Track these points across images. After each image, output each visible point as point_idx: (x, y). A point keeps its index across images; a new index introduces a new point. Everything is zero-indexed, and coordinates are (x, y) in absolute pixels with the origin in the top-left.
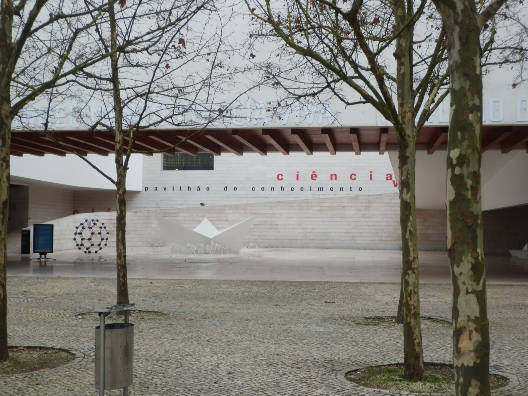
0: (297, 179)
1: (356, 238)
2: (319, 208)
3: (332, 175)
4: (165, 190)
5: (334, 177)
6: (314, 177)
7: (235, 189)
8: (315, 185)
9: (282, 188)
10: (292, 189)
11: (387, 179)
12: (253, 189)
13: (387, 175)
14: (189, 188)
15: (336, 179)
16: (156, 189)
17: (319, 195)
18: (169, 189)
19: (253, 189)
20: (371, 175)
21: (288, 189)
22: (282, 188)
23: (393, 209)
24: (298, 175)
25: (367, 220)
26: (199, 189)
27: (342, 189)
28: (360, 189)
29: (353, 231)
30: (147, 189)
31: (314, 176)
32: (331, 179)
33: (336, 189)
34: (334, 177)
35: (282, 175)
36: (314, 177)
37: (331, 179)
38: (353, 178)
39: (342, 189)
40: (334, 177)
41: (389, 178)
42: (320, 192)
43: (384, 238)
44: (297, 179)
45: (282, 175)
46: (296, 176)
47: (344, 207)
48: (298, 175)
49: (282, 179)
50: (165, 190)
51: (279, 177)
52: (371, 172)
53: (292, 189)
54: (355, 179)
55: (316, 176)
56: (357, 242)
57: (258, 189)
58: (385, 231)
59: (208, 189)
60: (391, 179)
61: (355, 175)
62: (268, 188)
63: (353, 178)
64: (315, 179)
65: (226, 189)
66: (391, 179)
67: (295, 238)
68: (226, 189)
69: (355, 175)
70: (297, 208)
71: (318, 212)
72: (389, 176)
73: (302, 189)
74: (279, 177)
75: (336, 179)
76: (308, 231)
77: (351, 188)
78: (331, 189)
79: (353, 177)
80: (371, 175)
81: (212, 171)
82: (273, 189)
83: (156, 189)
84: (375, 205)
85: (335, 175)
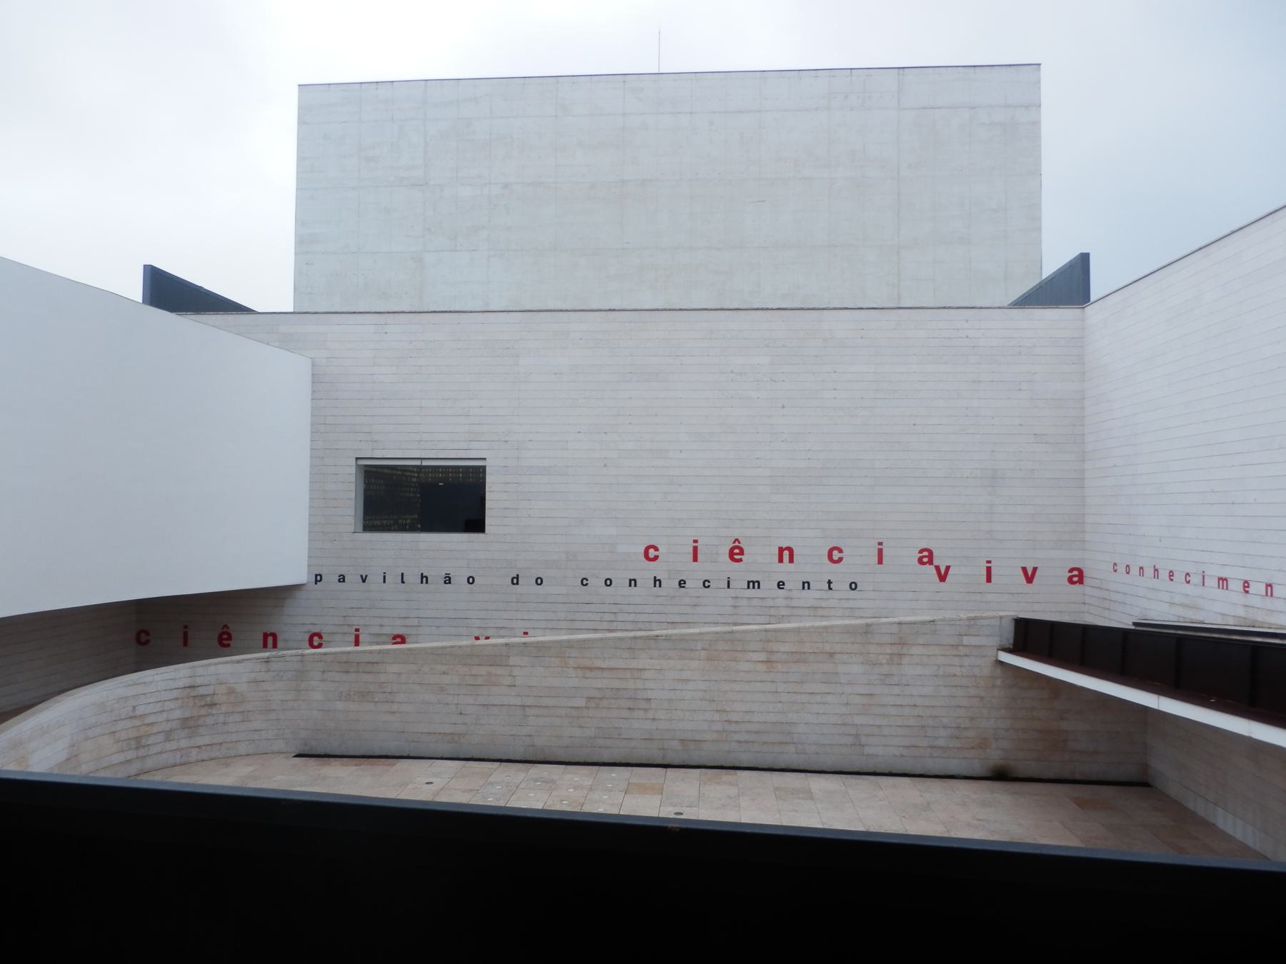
0: (695, 559)
1: (864, 740)
2: (763, 657)
3: (781, 550)
4: (364, 581)
5: (786, 553)
6: (736, 553)
7: (539, 581)
8: (740, 573)
9: (657, 582)
10: (682, 584)
11: (920, 561)
12: (584, 582)
13: (921, 552)
14: (424, 579)
15: (791, 560)
16: (342, 579)
17: (750, 598)
18: (375, 579)
19: (584, 582)
20: (880, 551)
21: (670, 584)
22: (657, 582)
23: (966, 661)
24: (695, 549)
25: (896, 690)
26: (448, 580)
27: (806, 585)
28: (853, 586)
29: (858, 720)
30: (318, 578)
31: (736, 551)
32: (781, 560)
33: (793, 584)
34: (786, 553)
35: (656, 549)
36: (736, 553)
37: (781, 560)
38: (835, 558)
39: (806, 585)
40: (786, 553)
41: (925, 560)
42: (751, 593)
43: (941, 742)
44: (695, 559)
45: (656, 549)
46: (691, 550)
47: (832, 654)
48: (695, 549)
49: (656, 558)
50: (364, 581)
51: (650, 553)
52: (880, 544)
53: (682, 584)
54: (840, 560)
55: (742, 553)
56: (867, 750)
57: (596, 582)
58: (945, 721)
59: (471, 580)
60: (930, 562)
61: (840, 551)
62: (621, 578)
63: (835, 558)
64: (740, 560)
65: (515, 580)
66: (930, 562)
67: (697, 738)
68: (515, 580)
69: (840, 551)
70: (703, 654)
71: (762, 667)
72: (926, 554)
73: (706, 584)
74: (650, 553)
75: (791, 560)
76: (734, 717)
77: (830, 582)
78: (781, 585)
79: (836, 555)
80: (880, 551)
81: (481, 535)
82: (632, 582)
83: (342, 579)
84: (915, 650)
85: (790, 550)
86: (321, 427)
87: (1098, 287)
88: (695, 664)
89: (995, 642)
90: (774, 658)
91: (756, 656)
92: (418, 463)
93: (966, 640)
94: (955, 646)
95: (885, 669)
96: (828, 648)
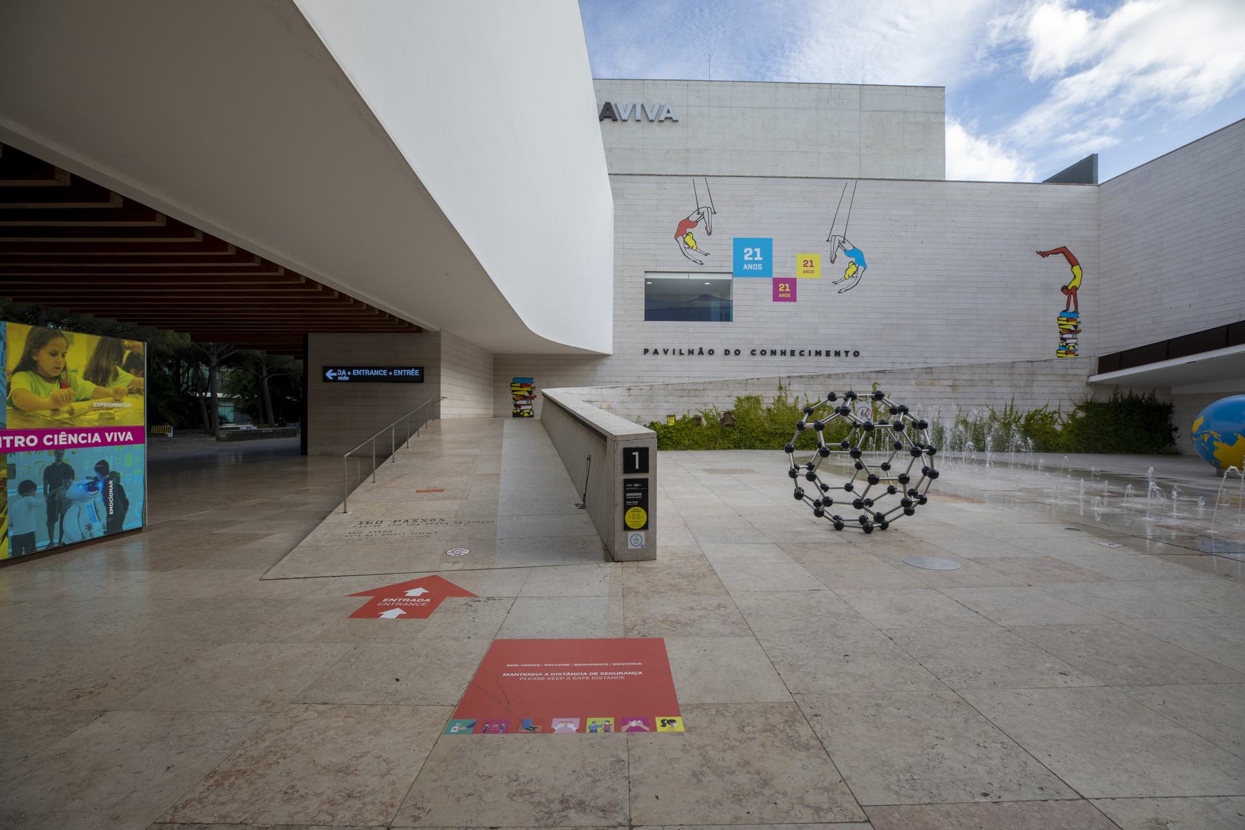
2: (950, 383)
23: (1070, 384)
25: (1029, 402)
47: (991, 381)
70: (914, 382)
71: (949, 389)
84: (1042, 378)
86: (621, 251)
87: (1103, 175)
88: (909, 388)
89: (1087, 372)
90: (957, 383)
91: (946, 383)
92: (685, 277)
93: (1070, 372)
94: (1064, 375)
95: (1022, 390)
96: (989, 377)
